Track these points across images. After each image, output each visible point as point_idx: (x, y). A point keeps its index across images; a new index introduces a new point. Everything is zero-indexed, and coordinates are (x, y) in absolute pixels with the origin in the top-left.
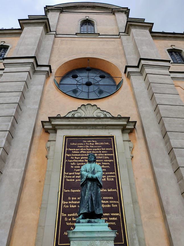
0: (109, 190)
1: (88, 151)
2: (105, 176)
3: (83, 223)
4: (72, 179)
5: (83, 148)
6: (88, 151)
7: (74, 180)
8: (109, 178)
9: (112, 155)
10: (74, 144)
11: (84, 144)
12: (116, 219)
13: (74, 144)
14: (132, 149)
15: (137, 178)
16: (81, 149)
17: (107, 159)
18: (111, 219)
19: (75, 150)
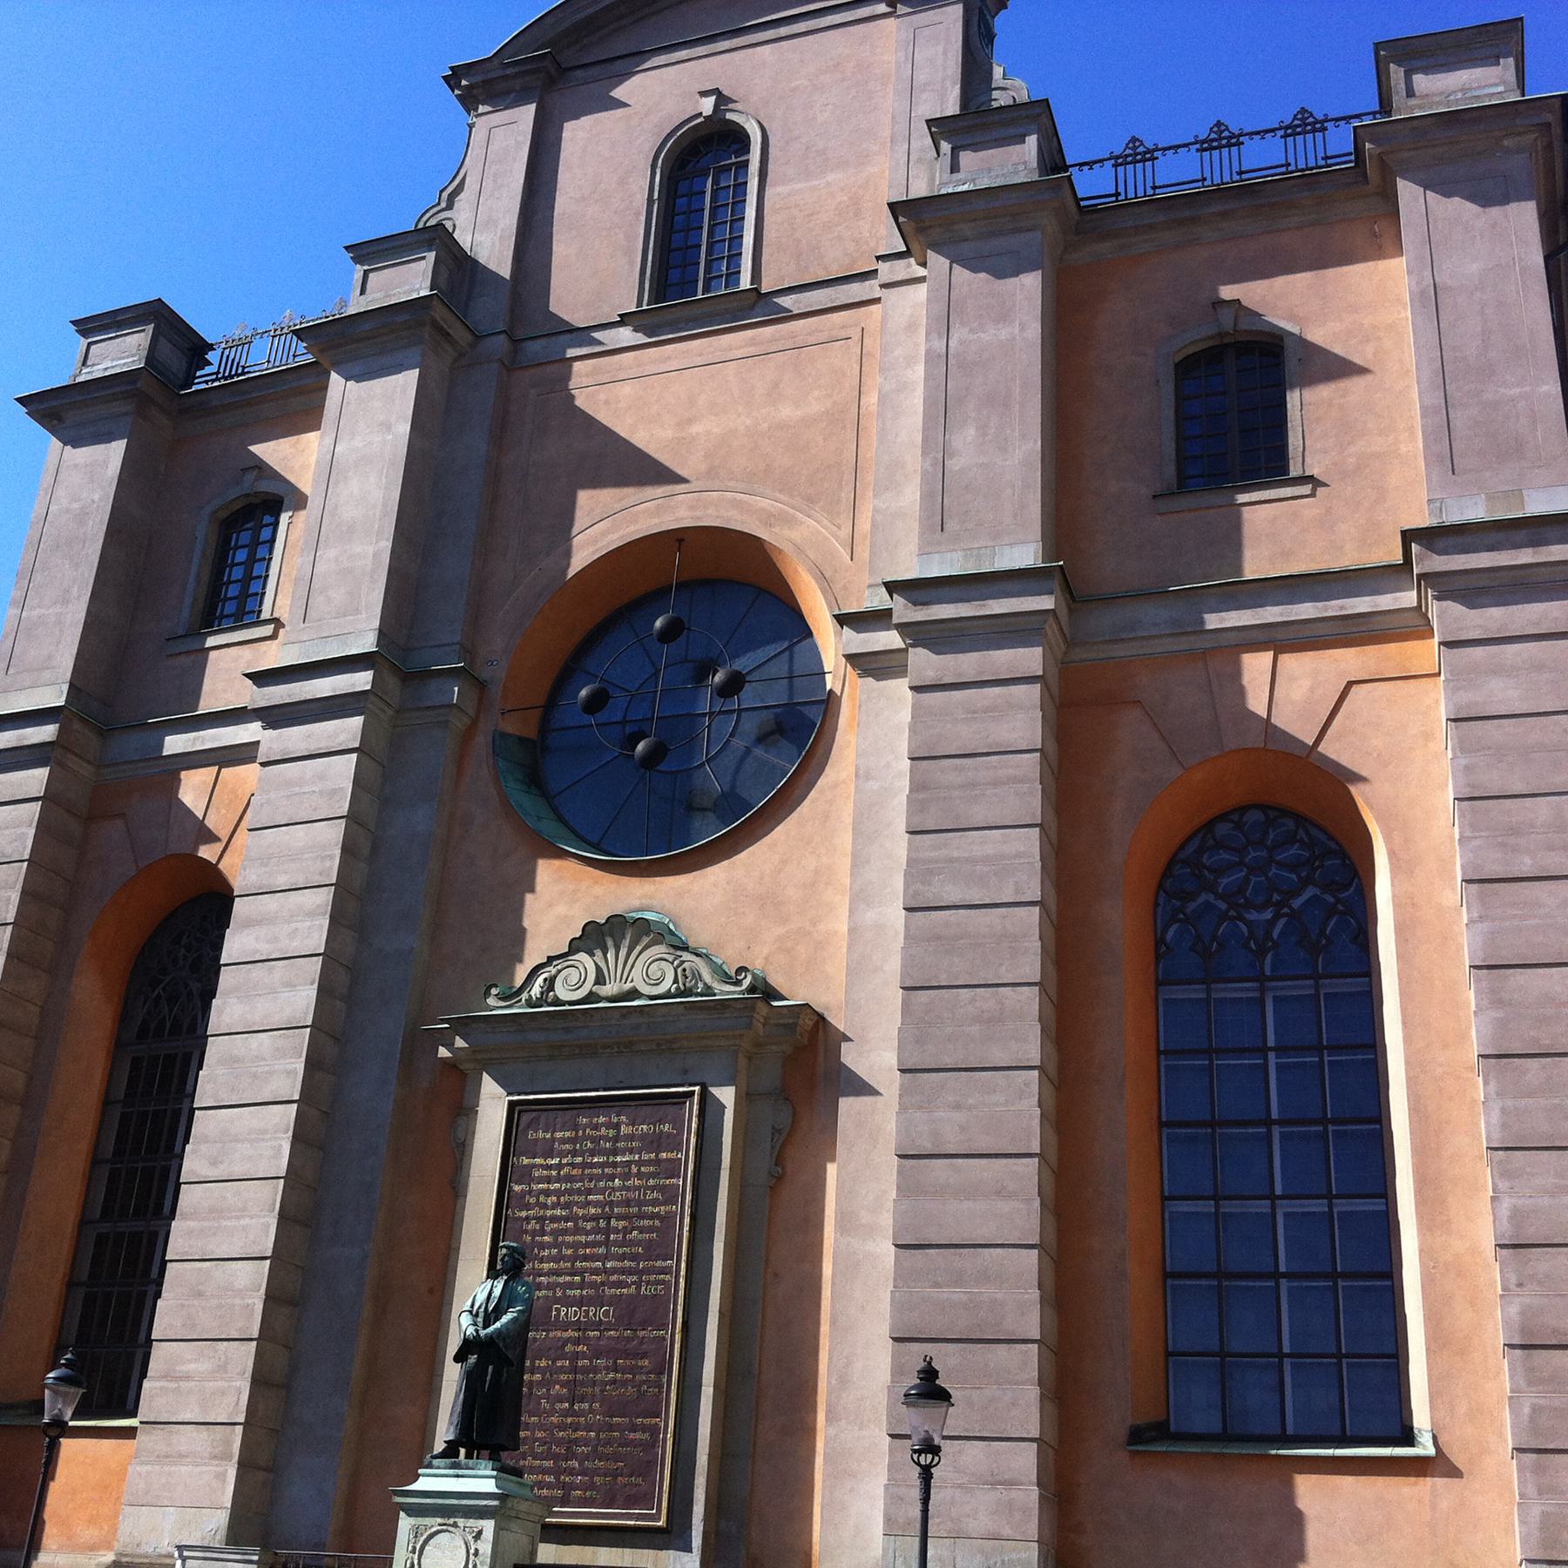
2: (635, 1278)
3: (438, 1468)
5: (574, 1153)
6: (592, 1166)
8: (648, 1283)
10: (541, 1134)
12: (646, 1436)
15: (776, 1275)
17: (655, 1203)
18: (632, 1436)
19: (541, 1166)
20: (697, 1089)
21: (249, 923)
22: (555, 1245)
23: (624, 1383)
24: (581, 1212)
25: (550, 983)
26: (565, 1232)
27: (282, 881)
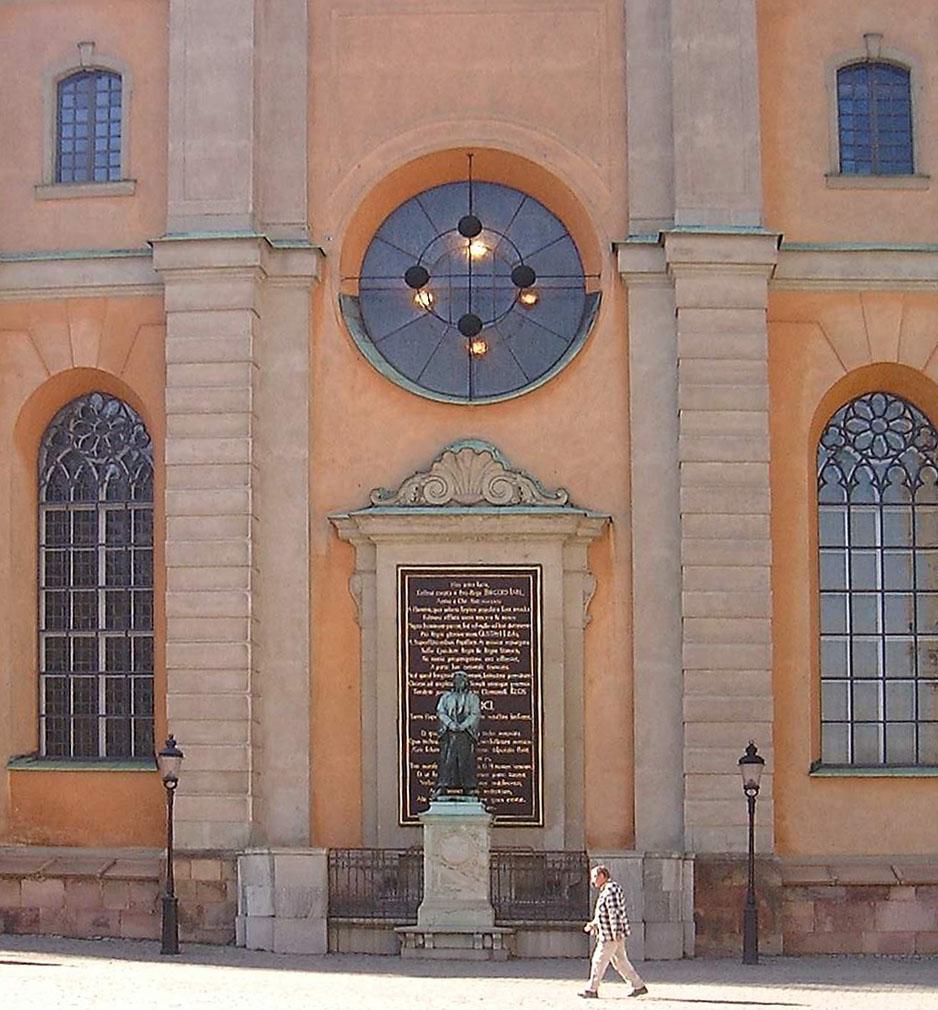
0: (512, 717)
1: (465, 614)
2: (506, 684)
4: (428, 689)
6: (465, 614)
7: (431, 692)
9: (528, 626)
10: (426, 593)
11: (455, 593)
13: (426, 593)
16: (446, 610)
17: (515, 639)
18: (514, 775)
20: (538, 569)
22: (445, 663)
23: (507, 746)
24: (462, 643)
25: (420, 490)
26: (451, 655)
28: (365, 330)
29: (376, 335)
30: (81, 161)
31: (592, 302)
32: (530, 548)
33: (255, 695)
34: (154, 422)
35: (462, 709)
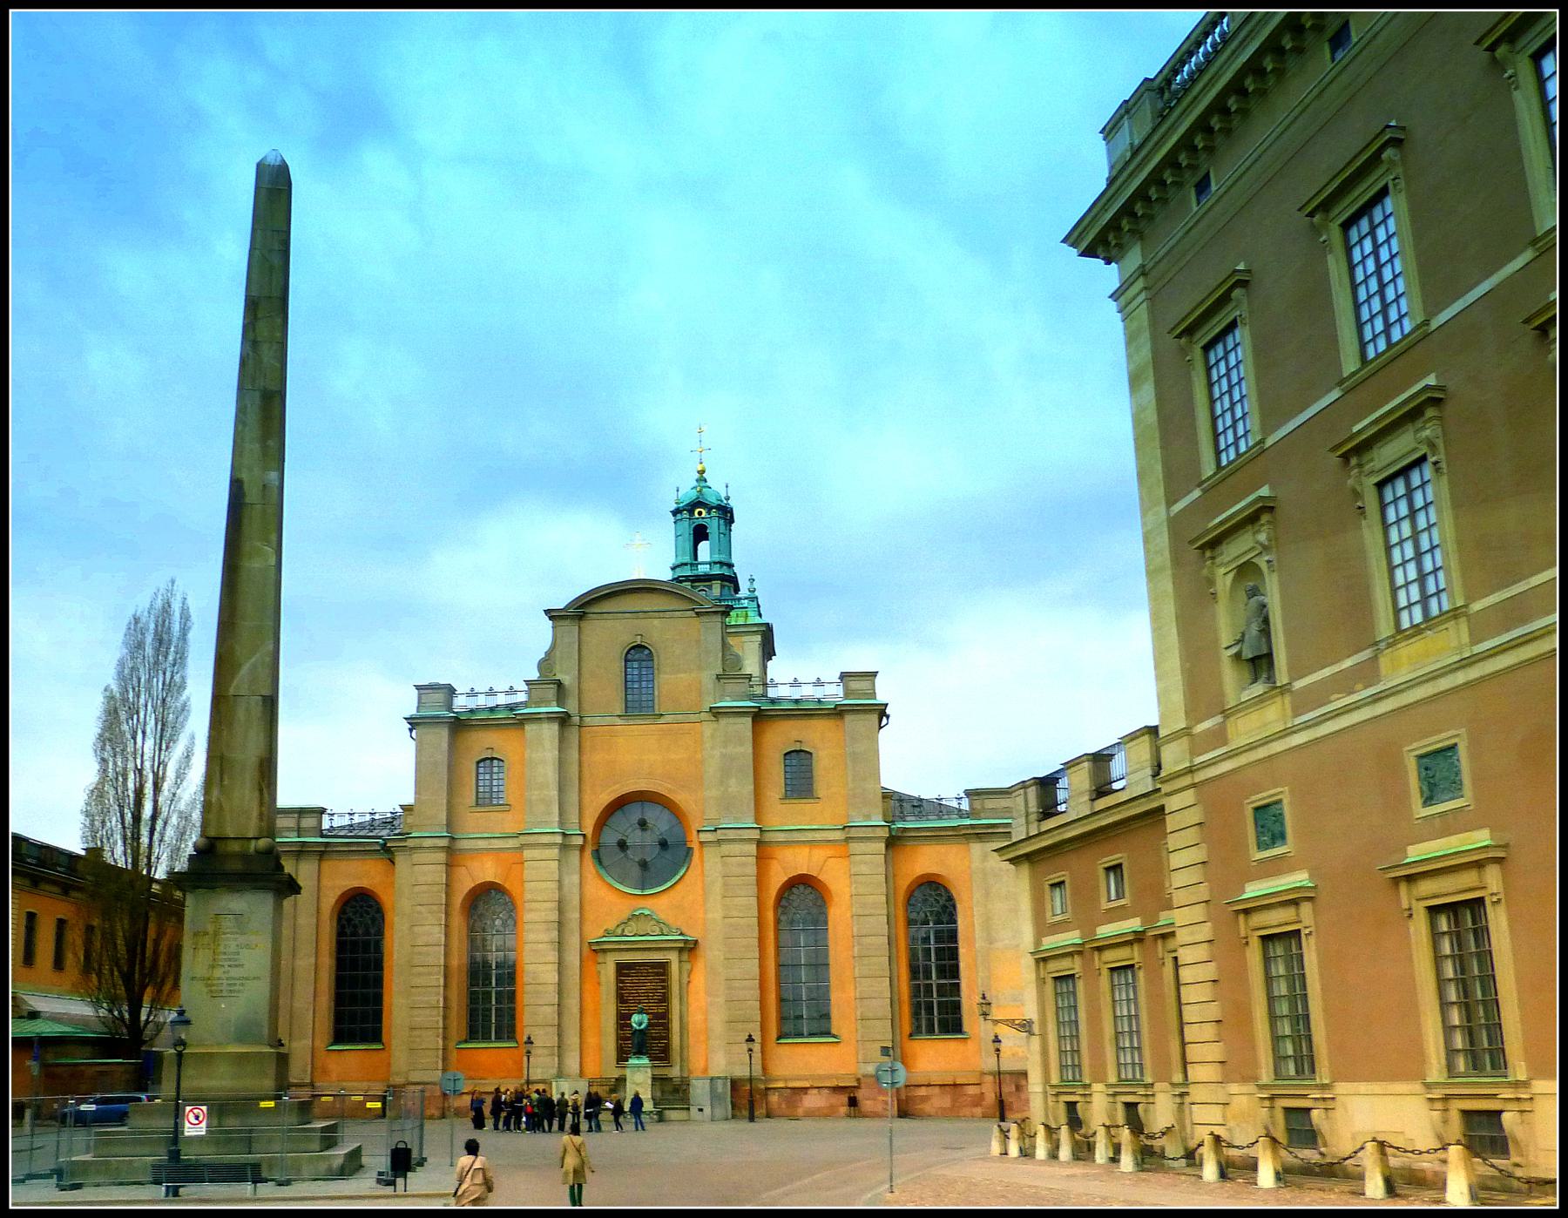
14: (690, 972)
21: (532, 910)
25: (623, 930)
27: (540, 899)
28: (600, 863)
29: (606, 863)
30: (487, 795)
31: (690, 849)
32: (665, 953)
33: (559, 1014)
34: (518, 903)
35: (638, 1020)
